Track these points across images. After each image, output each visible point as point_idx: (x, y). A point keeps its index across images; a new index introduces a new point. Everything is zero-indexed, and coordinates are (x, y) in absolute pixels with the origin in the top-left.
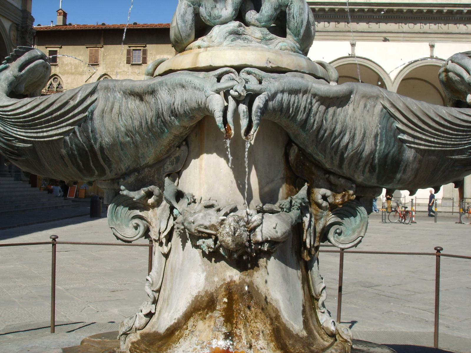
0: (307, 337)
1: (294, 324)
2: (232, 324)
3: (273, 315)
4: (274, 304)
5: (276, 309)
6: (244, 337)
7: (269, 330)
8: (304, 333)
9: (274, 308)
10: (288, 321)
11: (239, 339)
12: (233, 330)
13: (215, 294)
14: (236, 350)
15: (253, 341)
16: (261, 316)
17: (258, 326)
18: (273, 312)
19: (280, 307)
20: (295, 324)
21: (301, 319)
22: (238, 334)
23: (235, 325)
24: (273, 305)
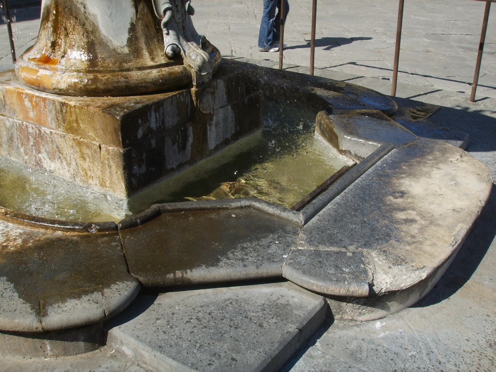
0: (127, 54)
1: (113, 40)
2: (57, 34)
3: (90, 29)
4: (91, 18)
5: (93, 23)
6: (63, 47)
7: (84, 43)
8: (126, 50)
9: (91, 22)
10: (106, 36)
11: (59, 48)
12: (56, 40)
13: (49, 6)
14: (54, 57)
15: (69, 51)
16: (79, 28)
17: (75, 38)
18: (89, 26)
19: (97, 22)
20: (115, 40)
21: (126, 36)
22: (59, 43)
23: (58, 35)
24: (91, 19)
